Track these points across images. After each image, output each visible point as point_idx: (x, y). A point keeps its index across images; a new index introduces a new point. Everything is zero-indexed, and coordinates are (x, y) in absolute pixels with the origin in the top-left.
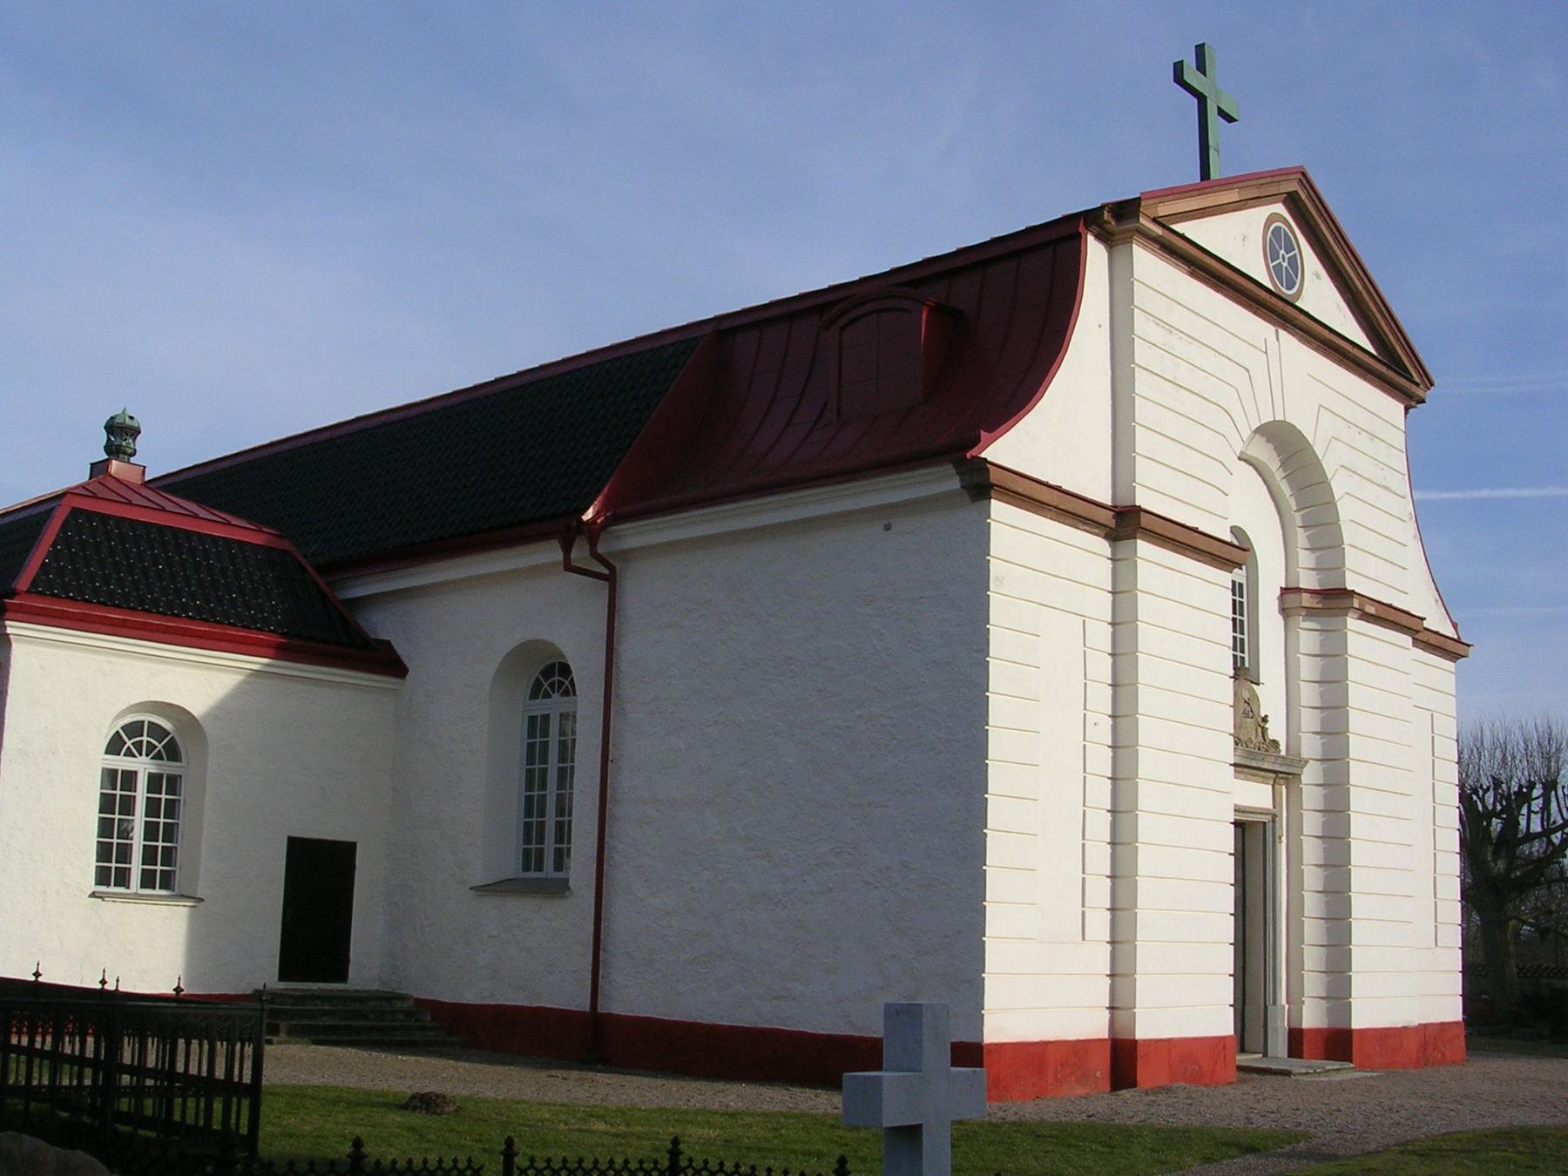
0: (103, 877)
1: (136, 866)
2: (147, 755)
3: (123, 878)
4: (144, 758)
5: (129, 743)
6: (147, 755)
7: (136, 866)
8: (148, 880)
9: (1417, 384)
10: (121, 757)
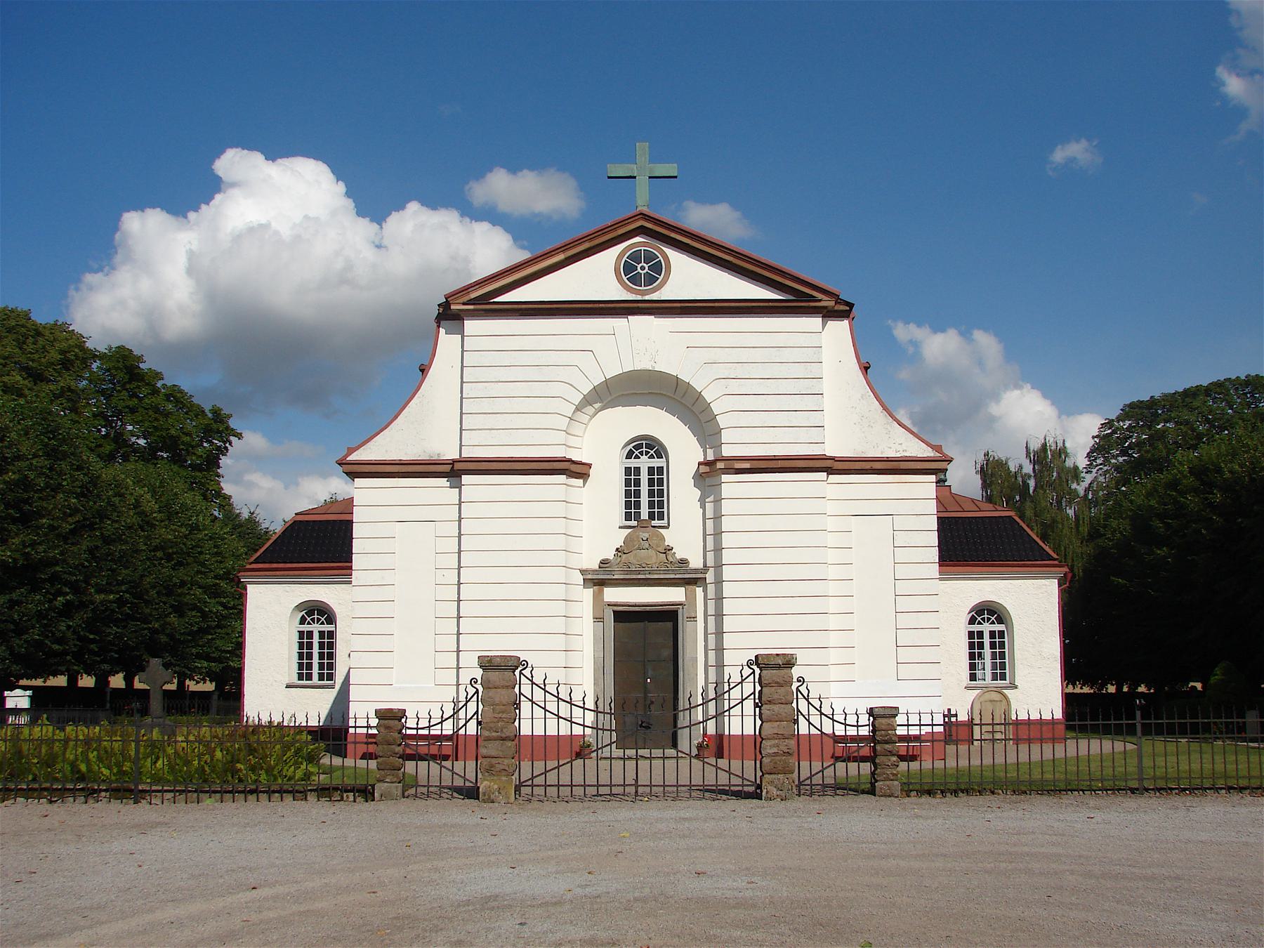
0: (300, 677)
1: (315, 671)
2: (317, 623)
3: (309, 677)
4: (316, 625)
5: (309, 619)
6: (317, 623)
7: (315, 671)
8: (321, 677)
9: (820, 301)
10: (305, 626)
